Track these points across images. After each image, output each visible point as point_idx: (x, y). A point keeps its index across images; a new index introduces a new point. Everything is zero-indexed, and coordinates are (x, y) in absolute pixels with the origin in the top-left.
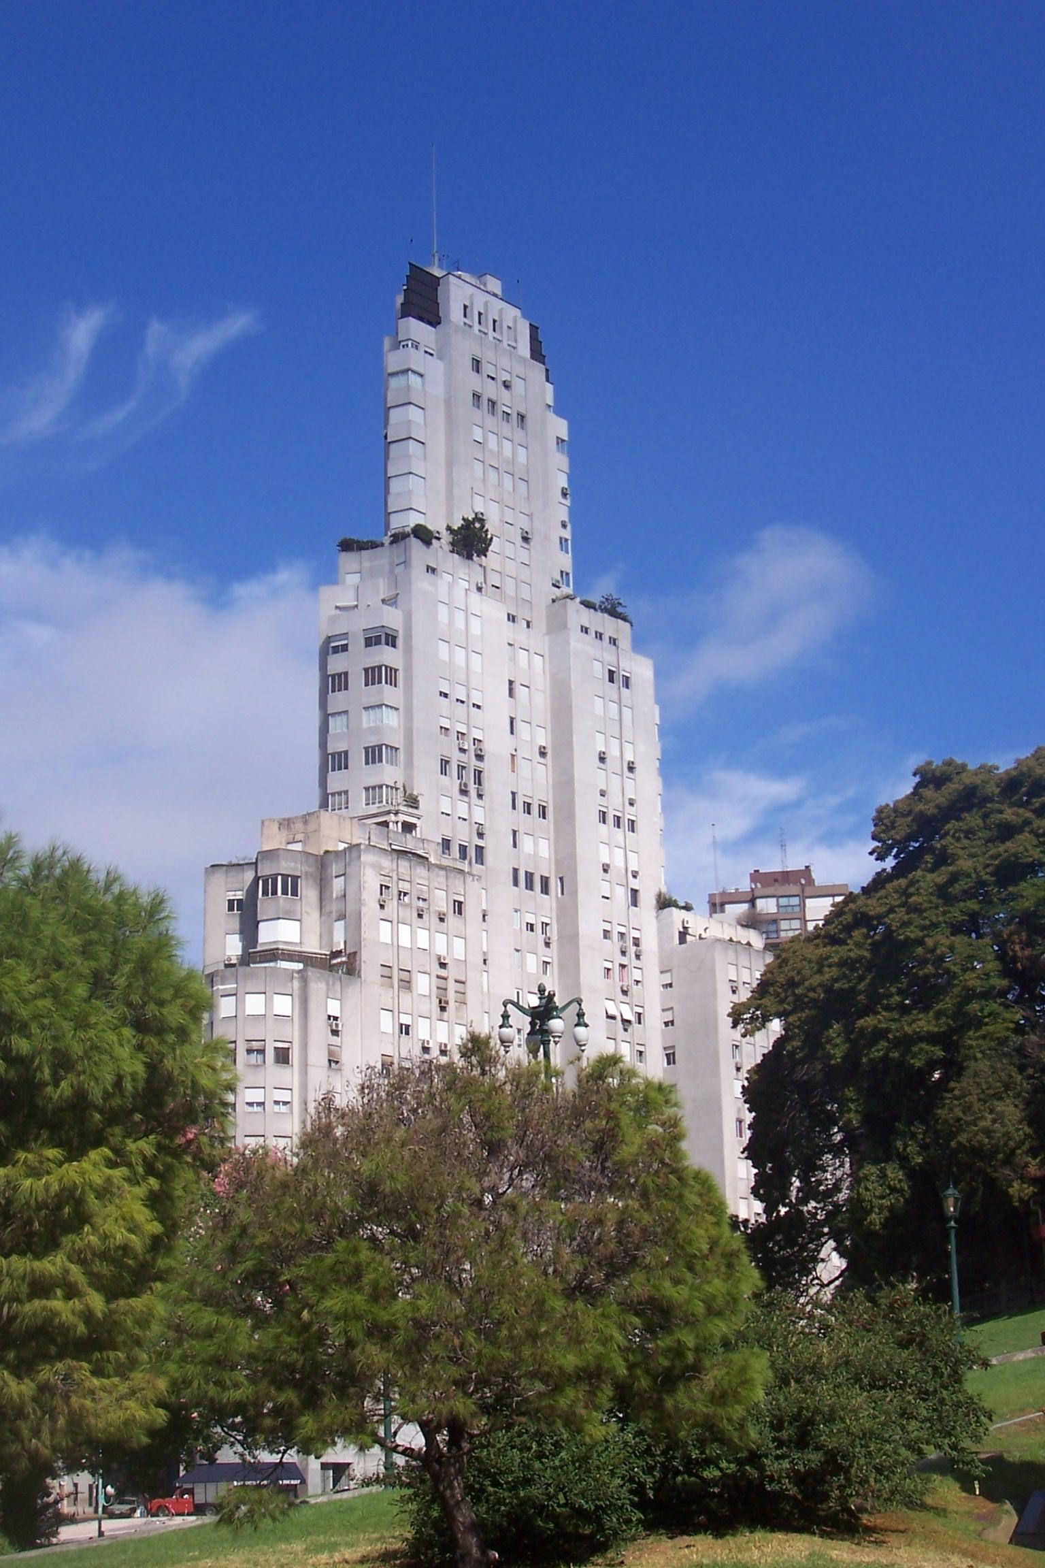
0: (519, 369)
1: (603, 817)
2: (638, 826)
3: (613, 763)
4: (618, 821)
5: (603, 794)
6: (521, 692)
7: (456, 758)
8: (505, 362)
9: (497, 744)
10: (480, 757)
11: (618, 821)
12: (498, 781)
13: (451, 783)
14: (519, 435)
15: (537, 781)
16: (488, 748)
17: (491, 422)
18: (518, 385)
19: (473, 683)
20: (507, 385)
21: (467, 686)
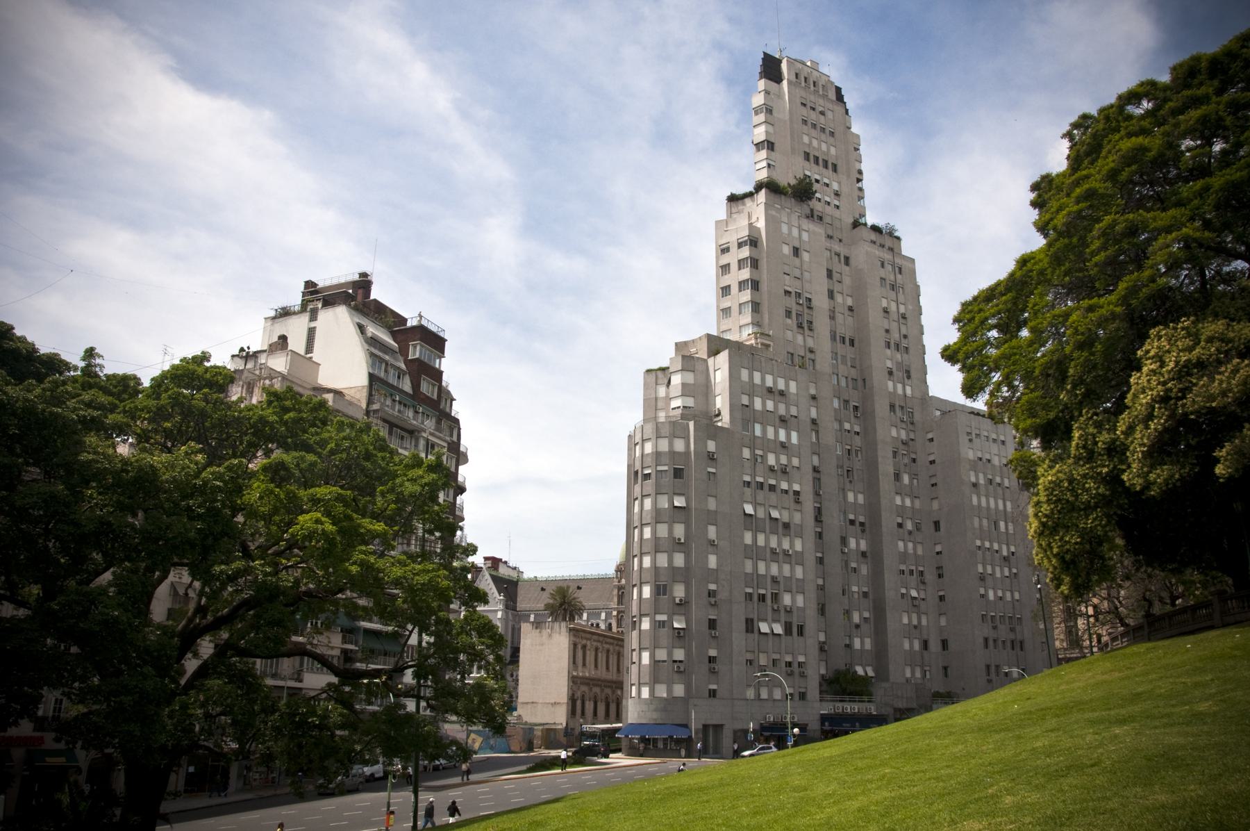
0: (830, 106)
1: (888, 345)
2: (911, 351)
3: (894, 316)
4: (897, 347)
5: (887, 331)
6: (836, 276)
7: (795, 308)
8: (821, 101)
9: (821, 303)
10: (810, 308)
11: (897, 347)
12: (822, 325)
13: (791, 322)
14: (831, 140)
15: (845, 325)
16: (814, 303)
17: (814, 133)
18: (830, 115)
19: (805, 267)
20: (822, 113)
21: (801, 269)
